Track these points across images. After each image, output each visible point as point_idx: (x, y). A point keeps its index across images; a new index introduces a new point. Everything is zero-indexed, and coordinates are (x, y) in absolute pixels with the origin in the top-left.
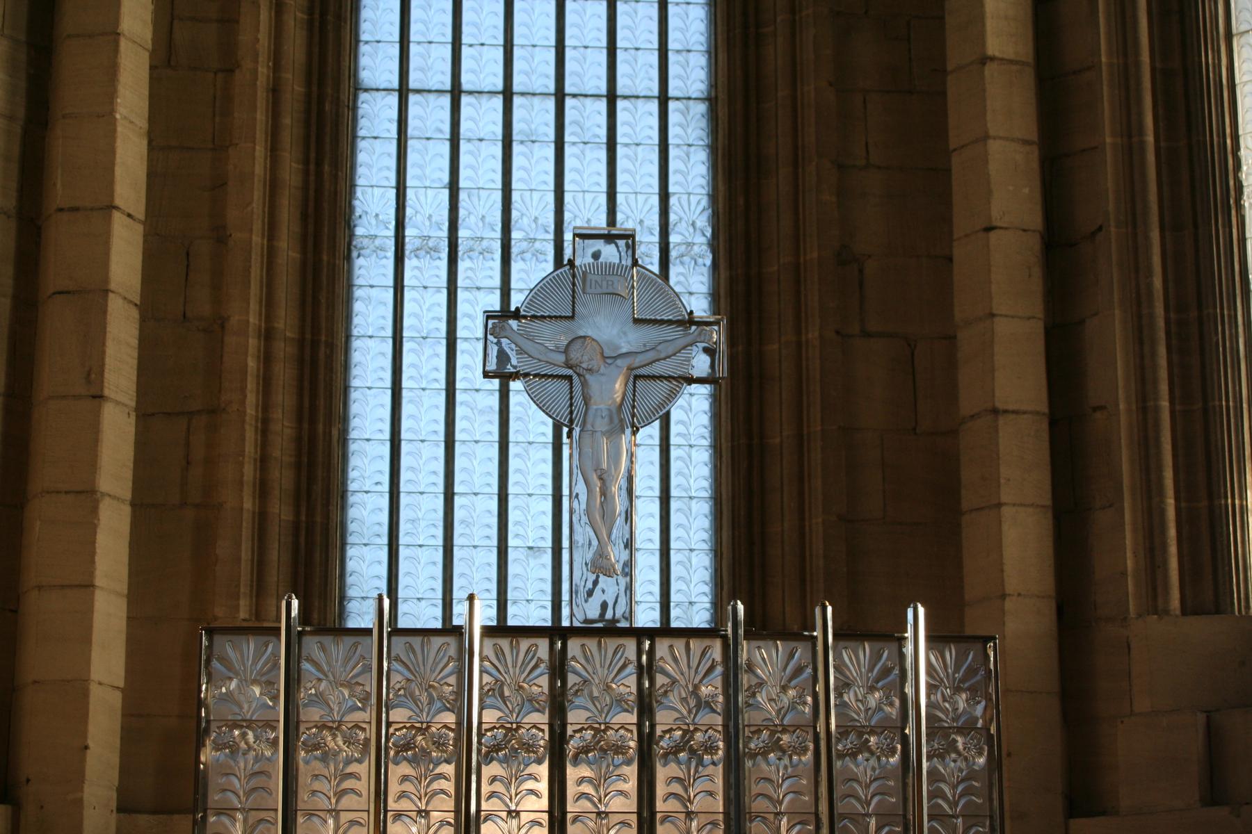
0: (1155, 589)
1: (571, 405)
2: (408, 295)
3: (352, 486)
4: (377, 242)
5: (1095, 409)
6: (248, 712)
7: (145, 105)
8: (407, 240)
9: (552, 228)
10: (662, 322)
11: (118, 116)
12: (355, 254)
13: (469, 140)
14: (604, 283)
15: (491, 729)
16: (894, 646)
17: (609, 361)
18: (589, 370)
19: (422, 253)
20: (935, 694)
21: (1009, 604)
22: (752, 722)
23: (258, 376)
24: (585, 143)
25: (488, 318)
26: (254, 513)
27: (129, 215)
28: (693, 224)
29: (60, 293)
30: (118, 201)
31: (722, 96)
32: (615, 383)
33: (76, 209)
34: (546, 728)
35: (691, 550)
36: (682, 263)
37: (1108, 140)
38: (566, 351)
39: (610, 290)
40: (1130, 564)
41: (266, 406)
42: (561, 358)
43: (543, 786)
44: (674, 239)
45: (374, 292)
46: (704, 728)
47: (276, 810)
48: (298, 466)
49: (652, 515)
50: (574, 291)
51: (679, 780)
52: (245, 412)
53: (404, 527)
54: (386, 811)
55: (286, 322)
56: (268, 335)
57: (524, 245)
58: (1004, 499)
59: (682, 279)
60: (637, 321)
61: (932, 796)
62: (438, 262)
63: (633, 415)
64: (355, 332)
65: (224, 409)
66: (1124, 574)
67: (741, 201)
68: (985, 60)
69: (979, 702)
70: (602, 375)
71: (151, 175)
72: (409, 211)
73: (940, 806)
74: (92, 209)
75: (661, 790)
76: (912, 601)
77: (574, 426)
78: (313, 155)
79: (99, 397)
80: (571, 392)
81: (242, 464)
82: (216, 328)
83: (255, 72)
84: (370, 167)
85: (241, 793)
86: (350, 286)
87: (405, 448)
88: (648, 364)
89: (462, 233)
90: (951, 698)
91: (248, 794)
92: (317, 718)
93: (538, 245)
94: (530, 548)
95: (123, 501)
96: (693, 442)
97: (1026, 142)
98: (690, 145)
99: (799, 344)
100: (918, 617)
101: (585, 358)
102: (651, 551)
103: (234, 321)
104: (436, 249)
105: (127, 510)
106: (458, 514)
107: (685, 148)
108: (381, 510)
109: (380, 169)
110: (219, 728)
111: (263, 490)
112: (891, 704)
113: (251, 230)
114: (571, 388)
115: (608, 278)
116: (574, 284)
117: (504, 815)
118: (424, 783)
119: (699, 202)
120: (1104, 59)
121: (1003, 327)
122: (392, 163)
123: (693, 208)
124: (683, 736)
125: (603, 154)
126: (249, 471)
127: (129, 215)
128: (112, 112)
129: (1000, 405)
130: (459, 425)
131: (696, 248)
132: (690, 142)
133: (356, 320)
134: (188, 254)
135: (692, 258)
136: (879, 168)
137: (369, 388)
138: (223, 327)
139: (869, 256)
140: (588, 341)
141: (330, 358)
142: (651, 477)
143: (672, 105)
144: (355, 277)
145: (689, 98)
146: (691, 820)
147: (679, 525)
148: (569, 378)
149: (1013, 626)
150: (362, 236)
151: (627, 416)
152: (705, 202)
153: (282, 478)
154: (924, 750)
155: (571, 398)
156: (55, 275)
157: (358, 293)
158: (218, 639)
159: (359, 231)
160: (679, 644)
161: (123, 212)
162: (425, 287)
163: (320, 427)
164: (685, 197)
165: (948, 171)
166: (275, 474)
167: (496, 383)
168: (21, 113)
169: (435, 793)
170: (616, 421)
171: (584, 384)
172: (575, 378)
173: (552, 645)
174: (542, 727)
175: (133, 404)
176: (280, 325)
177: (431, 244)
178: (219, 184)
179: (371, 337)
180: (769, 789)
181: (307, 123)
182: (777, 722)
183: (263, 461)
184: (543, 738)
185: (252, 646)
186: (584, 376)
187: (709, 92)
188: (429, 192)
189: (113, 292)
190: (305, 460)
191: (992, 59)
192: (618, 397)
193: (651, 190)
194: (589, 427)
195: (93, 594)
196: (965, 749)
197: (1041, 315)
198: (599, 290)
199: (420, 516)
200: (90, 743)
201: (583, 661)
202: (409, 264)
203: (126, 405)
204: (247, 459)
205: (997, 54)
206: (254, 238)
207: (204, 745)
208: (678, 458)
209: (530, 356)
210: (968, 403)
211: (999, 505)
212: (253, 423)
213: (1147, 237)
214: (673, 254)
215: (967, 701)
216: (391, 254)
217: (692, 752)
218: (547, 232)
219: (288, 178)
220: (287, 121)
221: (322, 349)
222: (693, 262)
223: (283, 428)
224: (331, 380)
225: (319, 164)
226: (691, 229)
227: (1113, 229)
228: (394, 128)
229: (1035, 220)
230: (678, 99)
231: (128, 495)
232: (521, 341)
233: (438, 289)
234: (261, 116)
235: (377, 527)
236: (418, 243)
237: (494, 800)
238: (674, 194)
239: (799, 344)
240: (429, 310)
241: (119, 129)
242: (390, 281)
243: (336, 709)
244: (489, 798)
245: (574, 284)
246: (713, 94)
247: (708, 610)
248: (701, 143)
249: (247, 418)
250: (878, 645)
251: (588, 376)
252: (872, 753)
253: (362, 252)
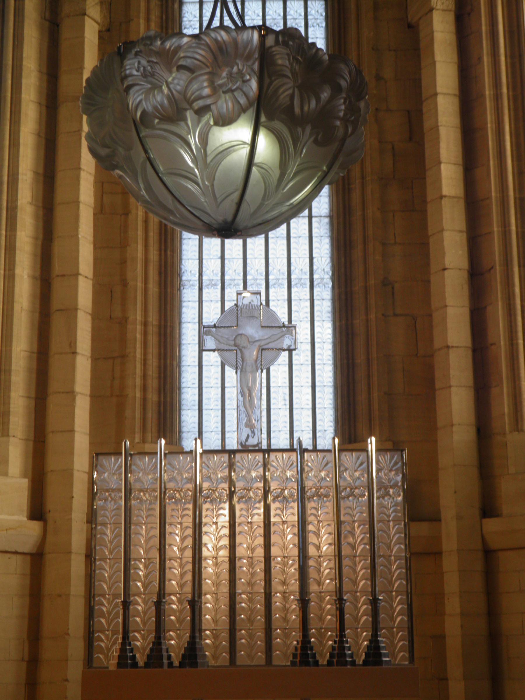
0: (517, 420)
2: (204, 304)
3: (183, 385)
4: (191, 283)
5: (492, 345)
6: (113, 486)
7: (92, 231)
8: (204, 281)
9: (264, 273)
10: (272, 327)
11: (80, 236)
12: (182, 288)
15: (206, 490)
16: (365, 454)
17: (251, 343)
18: (244, 347)
19: (210, 287)
20: (381, 472)
21: (455, 429)
22: (308, 485)
23: (141, 342)
24: (277, 237)
26: (141, 398)
27: (86, 277)
28: (324, 270)
29: (58, 310)
30: (81, 271)
31: (335, 215)
32: (253, 352)
33: (63, 276)
34: (228, 489)
35: (325, 408)
36: (319, 287)
37: (496, 229)
38: (234, 340)
40: (506, 410)
41: (145, 354)
42: (232, 343)
43: (226, 512)
44: (315, 276)
45: (190, 304)
46: (289, 488)
47: (122, 523)
48: (159, 378)
49: (308, 394)
50: (237, 316)
51: (280, 509)
52: (136, 357)
54: (165, 523)
55: (153, 318)
56: (145, 324)
57: (252, 282)
58: (452, 384)
59: (319, 293)
60: (262, 327)
61: (379, 513)
62: (216, 290)
63: (261, 365)
64: (183, 321)
65: (127, 356)
66: (504, 415)
67: (343, 260)
68: (442, 197)
69: (398, 476)
71: (95, 259)
72: (204, 269)
73: (383, 517)
74: (71, 275)
75: (272, 513)
76: (370, 435)
78: (163, 248)
79: (75, 353)
80: (237, 356)
81: (135, 379)
82: (123, 322)
83: (137, 214)
84: (188, 251)
85: (109, 517)
86: (180, 301)
87: (204, 368)
89: (227, 277)
90: (388, 473)
91: (112, 518)
92: (139, 487)
93: (258, 281)
95: (86, 395)
96: (325, 362)
97: (461, 231)
98: (322, 237)
99: (367, 320)
100: (372, 442)
102: (308, 409)
103: (131, 318)
104: (215, 285)
105: (88, 399)
107: (320, 238)
108: (195, 395)
109: (192, 252)
110: (101, 492)
111: (144, 388)
112: (363, 477)
113: (137, 281)
116: (237, 313)
117: (211, 523)
118: (180, 512)
119: (326, 260)
120: (493, 194)
121: (451, 312)
122: (197, 249)
123: (323, 263)
124: (281, 492)
125: (285, 242)
126: (138, 381)
127: (86, 277)
128: (77, 235)
129: (450, 344)
131: (325, 280)
132: (322, 235)
133: (183, 316)
134: (111, 292)
135: (323, 285)
136: (400, 244)
137: (189, 344)
138: (126, 321)
139: (396, 282)
140: (243, 336)
141: (172, 332)
142: (307, 378)
143: (314, 220)
144: (182, 298)
145: (321, 216)
146: (284, 524)
147: (320, 398)
149: (456, 437)
150: (185, 280)
151: (259, 366)
152: (328, 260)
153: (153, 383)
154: (375, 495)
155: (237, 358)
156: (56, 304)
157: (184, 304)
158: (100, 458)
159: (184, 278)
160: (279, 455)
161: (83, 276)
162: (211, 301)
163: (168, 362)
164: (320, 259)
165: (428, 244)
166: (149, 382)
168: (41, 236)
169: (184, 515)
170: (254, 367)
171: (242, 353)
173: (230, 456)
174: (226, 489)
175: (89, 355)
176: (150, 319)
177: (213, 283)
178: (123, 262)
179: (189, 322)
180: (314, 511)
181: (160, 234)
182: (318, 485)
183: (145, 376)
184: (226, 493)
185: (113, 459)
187: (330, 213)
188: (212, 261)
189: (79, 309)
190: (162, 375)
191: (445, 196)
192: (254, 357)
193: (305, 256)
194: (244, 370)
195: (74, 434)
196: (393, 494)
197: (468, 305)
199: (211, 397)
200: (74, 495)
201: (241, 462)
202: (205, 291)
203: (86, 356)
204: (137, 376)
205: (447, 194)
206: (138, 284)
207: (95, 499)
208: (319, 369)
210: (437, 343)
211: (450, 387)
212: (140, 361)
213: (512, 271)
214: (315, 283)
215: (394, 475)
216: (197, 287)
217: (285, 497)
218: (262, 275)
219: (152, 258)
220: (151, 234)
221: (169, 328)
222: (324, 286)
223: (153, 362)
224: (173, 341)
225: (166, 251)
226: (323, 272)
227: (498, 268)
229: (464, 264)
230: (316, 217)
231: (88, 392)
233: (217, 302)
234: (140, 232)
235: (193, 402)
236: (208, 282)
237: (207, 518)
238: (315, 257)
239: (367, 320)
240: (213, 310)
241: (81, 241)
242: (197, 299)
243: (145, 483)
244: (206, 517)
245: (237, 313)
246: (332, 214)
247: (332, 433)
248: (327, 235)
249: (137, 359)
250: (358, 453)
251: (243, 350)
252: (355, 497)
253: (185, 287)
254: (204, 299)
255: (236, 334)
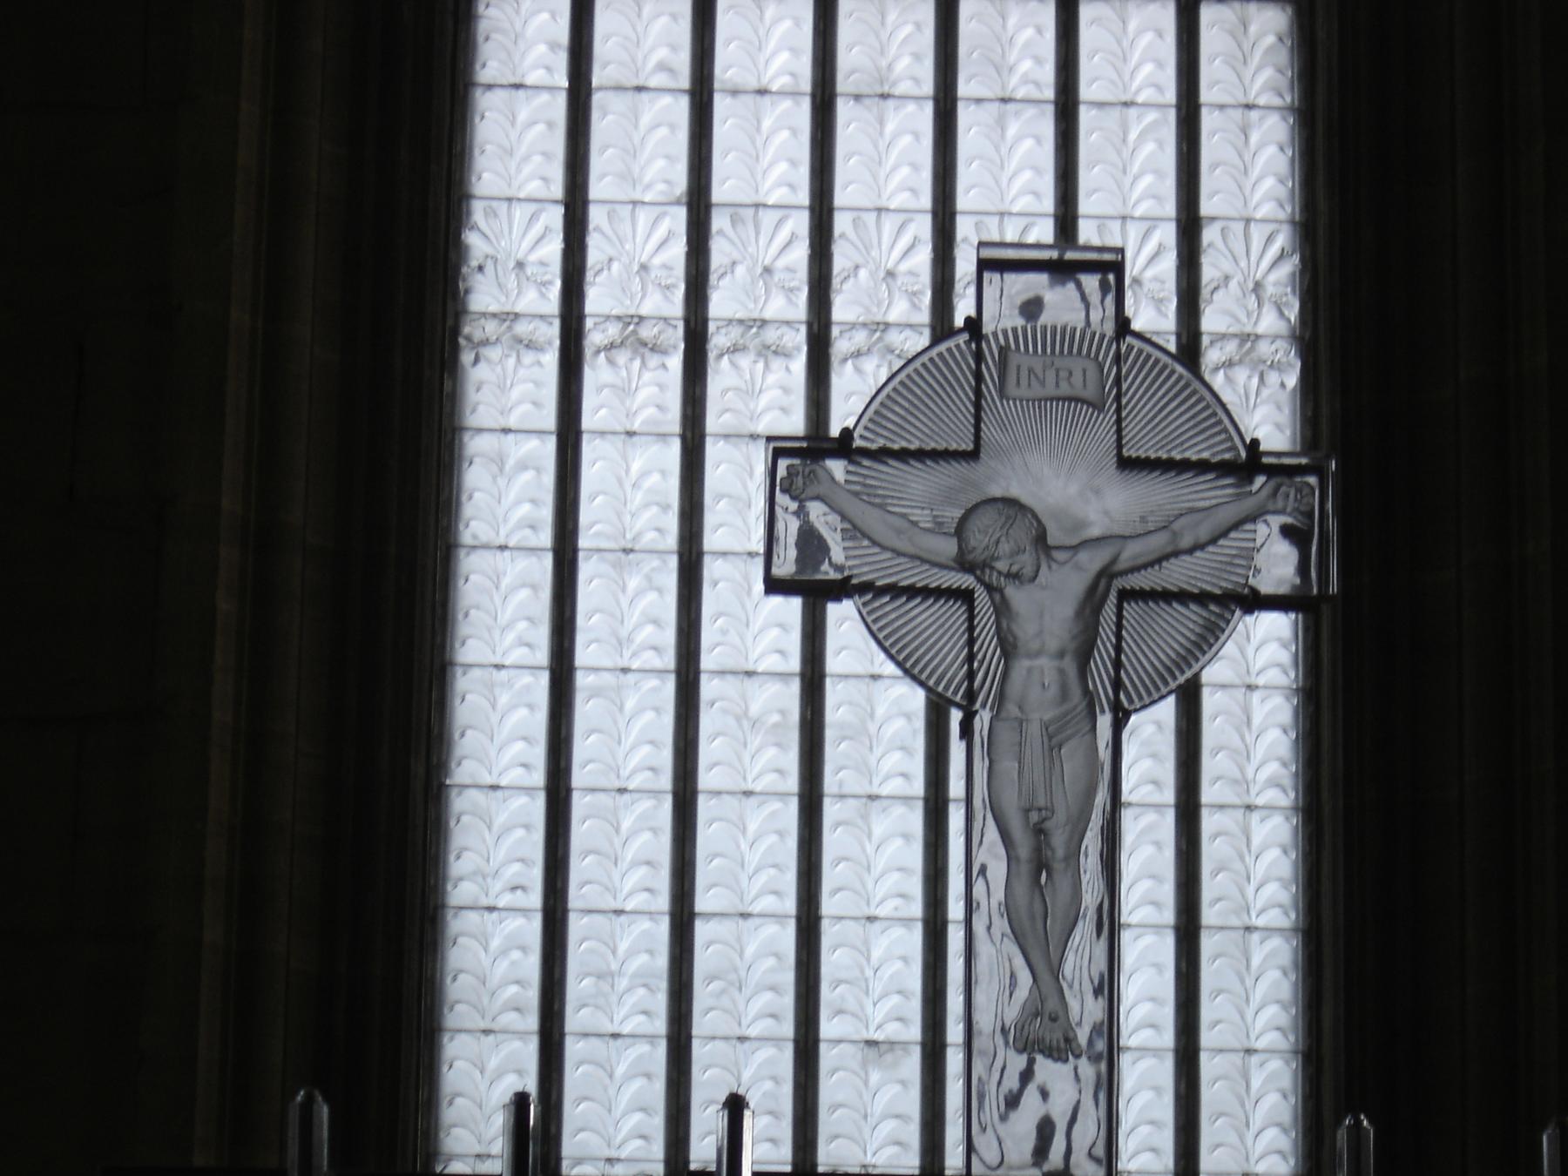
1: (971, 658)
2: (590, 450)
10: (1183, 466)
13: (735, 92)
14: (1050, 377)
25: (778, 453)
28: (1258, 287)
38: (960, 531)
39: (1065, 389)
42: (948, 548)
50: (978, 393)
53: (577, 987)
60: (1127, 464)
63: (1117, 684)
70: (1044, 588)
77: (978, 705)
88: (1151, 564)
94: (871, 1043)
101: (1005, 547)
106: (704, 959)
114: (971, 618)
115: (1058, 362)
116: (979, 377)
119: (1270, 240)
125: (1046, 127)
130: (709, 750)
131: (1264, 348)
148: (966, 596)
150: (484, 315)
151: (1103, 689)
155: (971, 642)
157: (476, 446)
164: (1238, 227)
167: (795, 604)
171: (1002, 609)
172: (981, 596)
186: (1001, 591)
194: (1011, 709)
198: (1037, 391)
202: (595, 375)
209: (875, 543)
228: (561, 62)
232: (856, 509)
238: (1213, 219)
245: (979, 377)
251: (1011, 591)
254: (588, 421)
255: (975, 498)
